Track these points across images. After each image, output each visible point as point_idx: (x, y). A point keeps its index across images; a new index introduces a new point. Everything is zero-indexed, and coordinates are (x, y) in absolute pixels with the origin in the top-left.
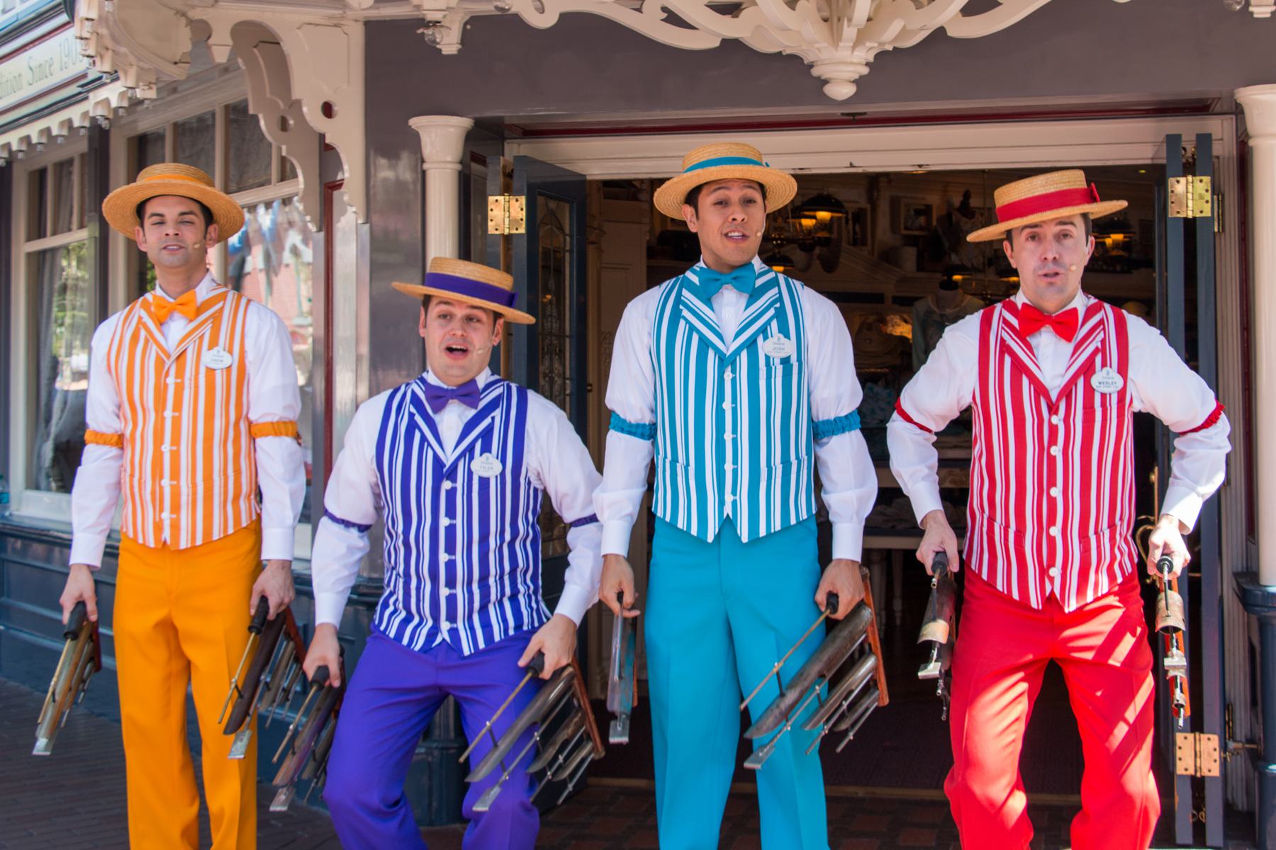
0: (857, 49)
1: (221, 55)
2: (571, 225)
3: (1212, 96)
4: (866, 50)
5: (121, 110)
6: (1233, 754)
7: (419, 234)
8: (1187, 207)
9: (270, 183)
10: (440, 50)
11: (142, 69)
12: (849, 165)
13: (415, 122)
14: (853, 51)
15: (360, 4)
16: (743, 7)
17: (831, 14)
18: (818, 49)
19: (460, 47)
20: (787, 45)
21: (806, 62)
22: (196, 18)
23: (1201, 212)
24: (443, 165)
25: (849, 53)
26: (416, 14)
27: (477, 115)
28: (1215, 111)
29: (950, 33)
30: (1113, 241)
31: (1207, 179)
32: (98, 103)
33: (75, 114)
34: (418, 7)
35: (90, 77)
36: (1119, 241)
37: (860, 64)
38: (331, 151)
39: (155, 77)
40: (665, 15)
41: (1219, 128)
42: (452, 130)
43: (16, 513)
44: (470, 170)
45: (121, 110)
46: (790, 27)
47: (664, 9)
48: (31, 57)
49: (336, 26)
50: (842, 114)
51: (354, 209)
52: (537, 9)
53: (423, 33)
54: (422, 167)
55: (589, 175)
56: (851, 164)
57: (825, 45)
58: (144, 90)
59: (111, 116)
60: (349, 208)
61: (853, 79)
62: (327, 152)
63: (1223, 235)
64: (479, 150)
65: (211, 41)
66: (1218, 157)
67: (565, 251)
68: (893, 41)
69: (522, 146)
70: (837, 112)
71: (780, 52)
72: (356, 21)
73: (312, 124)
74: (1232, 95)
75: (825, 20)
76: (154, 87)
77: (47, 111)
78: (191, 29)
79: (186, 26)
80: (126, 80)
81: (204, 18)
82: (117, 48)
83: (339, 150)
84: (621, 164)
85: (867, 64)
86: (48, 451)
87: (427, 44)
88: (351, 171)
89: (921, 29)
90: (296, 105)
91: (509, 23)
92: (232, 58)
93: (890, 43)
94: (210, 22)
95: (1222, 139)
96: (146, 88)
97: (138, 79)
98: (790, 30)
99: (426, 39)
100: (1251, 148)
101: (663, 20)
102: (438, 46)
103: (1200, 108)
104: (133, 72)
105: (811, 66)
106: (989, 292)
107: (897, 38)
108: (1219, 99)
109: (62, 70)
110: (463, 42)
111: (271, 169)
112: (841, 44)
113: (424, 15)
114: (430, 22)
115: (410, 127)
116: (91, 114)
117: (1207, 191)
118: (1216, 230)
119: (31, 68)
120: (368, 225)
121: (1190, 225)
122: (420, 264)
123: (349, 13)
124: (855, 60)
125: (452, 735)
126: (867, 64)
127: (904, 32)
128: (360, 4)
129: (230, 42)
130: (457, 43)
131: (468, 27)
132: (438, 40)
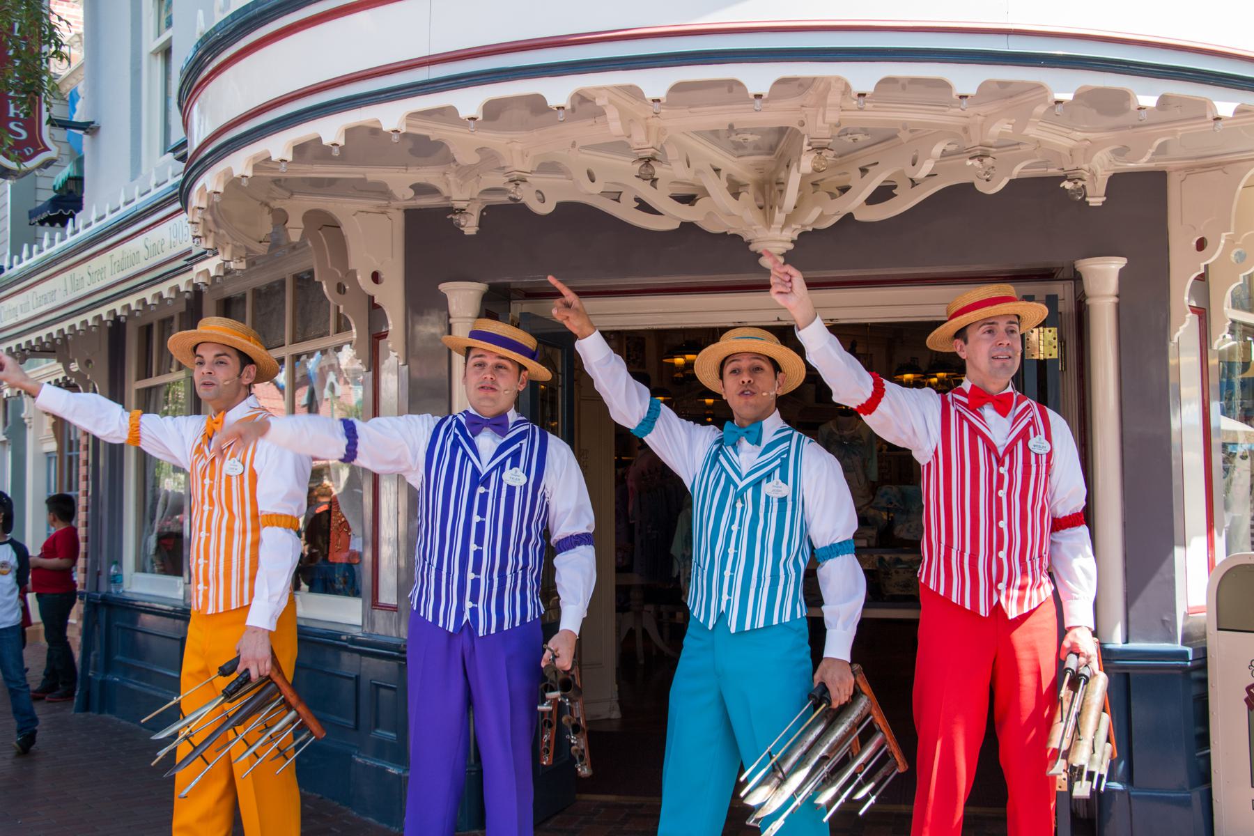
0: (785, 230)
1: (295, 236)
2: (562, 366)
5: (218, 278)
7: (446, 374)
8: (1039, 351)
9: (329, 335)
10: (463, 231)
11: (235, 246)
12: (776, 319)
13: (444, 287)
14: (782, 231)
15: (404, 196)
16: (697, 198)
18: (755, 230)
19: (478, 229)
21: (745, 240)
22: (276, 207)
23: (1050, 355)
25: (778, 233)
26: (445, 204)
27: (491, 281)
31: (1054, 330)
32: (200, 273)
33: (182, 282)
34: (448, 198)
35: (194, 253)
37: (787, 241)
38: (376, 310)
39: (245, 253)
41: (1062, 290)
42: (472, 293)
43: (127, 590)
45: (218, 278)
46: (733, 211)
47: (637, 199)
48: (147, 238)
49: (383, 213)
51: (396, 354)
52: (539, 200)
53: (452, 218)
54: (448, 322)
56: (778, 318)
57: (761, 227)
59: (209, 283)
60: (391, 353)
62: (375, 310)
63: (1065, 373)
64: (493, 309)
65: (287, 225)
66: (1061, 313)
67: (557, 386)
68: (812, 224)
69: (524, 305)
71: (726, 232)
72: (398, 209)
73: (364, 289)
74: (1074, 265)
75: (761, 208)
76: (244, 260)
77: (159, 280)
79: (269, 214)
80: (223, 255)
81: (282, 207)
82: (216, 231)
83: (385, 309)
85: (793, 242)
86: (152, 541)
88: (395, 323)
89: (835, 214)
90: (354, 273)
91: (518, 210)
92: (303, 236)
93: (809, 225)
94: (286, 210)
95: (1064, 299)
96: (238, 261)
97: (232, 257)
98: (734, 215)
100: (1088, 306)
101: (636, 208)
102: (462, 229)
103: (1046, 275)
104: (229, 249)
105: (749, 243)
107: (818, 220)
108: (1063, 268)
109: (171, 248)
110: (480, 225)
111: (329, 324)
112: (772, 226)
113: (453, 204)
114: (457, 209)
116: (194, 282)
117: (1055, 339)
118: (1060, 369)
119: (147, 247)
120: (407, 366)
121: (1042, 364)
123: (393, 203)
124: (785, 239)
125: (472, 761)
126: (793, 242)
127: (821, 217)
128: (404, 196)
129: (303, 226)
131: (485, 214)
132: (463, 224)
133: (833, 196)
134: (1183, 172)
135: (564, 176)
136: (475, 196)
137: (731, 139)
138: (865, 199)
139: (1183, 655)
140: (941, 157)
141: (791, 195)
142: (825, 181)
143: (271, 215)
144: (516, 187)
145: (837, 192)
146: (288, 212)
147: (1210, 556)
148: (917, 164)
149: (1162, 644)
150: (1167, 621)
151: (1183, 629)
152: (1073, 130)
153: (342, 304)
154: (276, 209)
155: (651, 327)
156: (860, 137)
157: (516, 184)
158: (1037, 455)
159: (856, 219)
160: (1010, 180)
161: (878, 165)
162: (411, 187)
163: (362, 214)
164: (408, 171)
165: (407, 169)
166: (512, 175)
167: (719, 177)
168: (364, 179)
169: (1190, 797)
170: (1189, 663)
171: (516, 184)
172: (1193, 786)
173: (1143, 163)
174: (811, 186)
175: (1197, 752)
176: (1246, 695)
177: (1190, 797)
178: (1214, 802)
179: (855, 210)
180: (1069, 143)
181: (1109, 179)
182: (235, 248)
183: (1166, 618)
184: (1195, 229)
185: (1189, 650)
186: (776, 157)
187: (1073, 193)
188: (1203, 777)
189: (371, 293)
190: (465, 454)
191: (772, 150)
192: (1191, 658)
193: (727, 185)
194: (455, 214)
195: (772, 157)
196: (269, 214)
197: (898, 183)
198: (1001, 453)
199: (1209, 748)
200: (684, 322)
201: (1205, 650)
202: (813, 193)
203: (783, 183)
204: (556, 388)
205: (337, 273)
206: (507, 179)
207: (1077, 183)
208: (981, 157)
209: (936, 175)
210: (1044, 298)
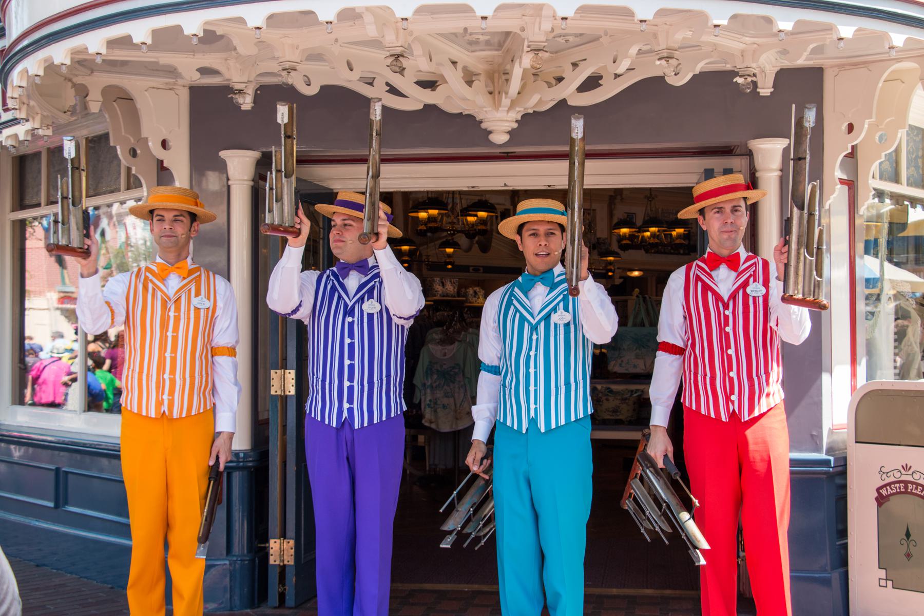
0: (511, 112)
3: (734, 144)
4: (516, 112)
6: (742, 560)
12: (503, 185)
13: (223, 154)
16: (438, 84)
17: (494, 90)
18: (486, 111)
19: (253, 105)
20: (466, 109)
21: (477, 119)
22: (78, 82)
24: (241, 182)
25: (505, 114)
27: (264, 150)
28: (736, 153)
29: (570, 103)
30: (677, 233)
36: (681, 233)
37: (512, 121)
39: (51, 122)
40: (388, 88)
42: (248, 159)
44: (259, 186)
46: (469, 98)
47: (387, 84)
49: (170, 89)
50: (500, 153)
54: (227, 183)
55: (335, 189)
56: (505, 184)
57: (490, 109)
58: (44, 129)
61: (507, 131)
65: (88, 98)
67: (320, 238)
70: (497, 151)
71: (461, 113)
72: (184, 86)
73: (153, 153)
75: (491, 93)
76: (51, 128)
78: (75, 90)
79: (72, 88)
81: (84, 82)
84: (355, 182)
85: (517, 121)
87: (235, 104)
93: (531, 108)
96: (45, 128)
97: (42, 123)
98: (469, 100)
99: (234, 101)
104: (38, 118)
105: (481, 122)
106: (593, 267)
110: (255, 102)
112: (500, 109)
113: (233, 85)
114: (236, 90)
115: (220, 156)
122: (226, 246)
123: (180, 81)
126: (517, 121)
128: (191, 77)
129: (101, 99)
130: (251, 103)
133: (550, 85)
134: (836, 68)
135: (327, 64)
136: (252, 79)
137: (465, 38)
138: (576, 87)
139: (826, 463)
140: (637, 54)
141: (515, 84)
142: (544, 72)
143: (73, 89)
144: (288, 75)
145: (554, 82)
146: (89, 88)
147: (853, 383)
148: (617, 61)
149: (810, 454)
150: (815, 435)
151: (827, 444)
152: (743, 35)
153: (134, 166)
154: (78, 84)
155: (399, 190)
156: (571, 39)
157: (288, 72)
158: (754, 298)
159: (569, 104)
160: (694, 75)
161: (587, 60)
162: (197, 70)
163: (154, 89)
164: (196, 57)
165: (194, 55)
166: (284, 65)
167: (456, 69)
168: (157, 63)
169: (831, 577)
170: (831, 469)
171: (288, 72)
172: (833, 568)
173: (801, 62)
174: (532, 75)
175: (838, 541)
176: (876, 495)
177: (831, 577)
178: (850, 581)
179: (568, 96)
180: (742, 46)
181: (776, 74)
182: (44, 118)
183: (814, 433)
184: (844, 117)
185: (832, 458)
186: (502, 53)
187: (744, 87)
188: (842, 560)
189: (161, 158)
190: (340, 297)
191: (500, 45)
192: (832, 466)
193: (462, 75)
194: (236, 94)
195: (499, 53)
196: (72, 88)
197: (603, 74)
198: (726, 299)
199: (847, 539)
200: (426, 186)
201: (845, 459)
202: (534, 82)
203: (508, 73)
204: (318, 240)
205: (130, 140)
206: (280, 68)
207: (746, 79)
208: (668, 58)
209: (634, 69)
210: (722, 171)
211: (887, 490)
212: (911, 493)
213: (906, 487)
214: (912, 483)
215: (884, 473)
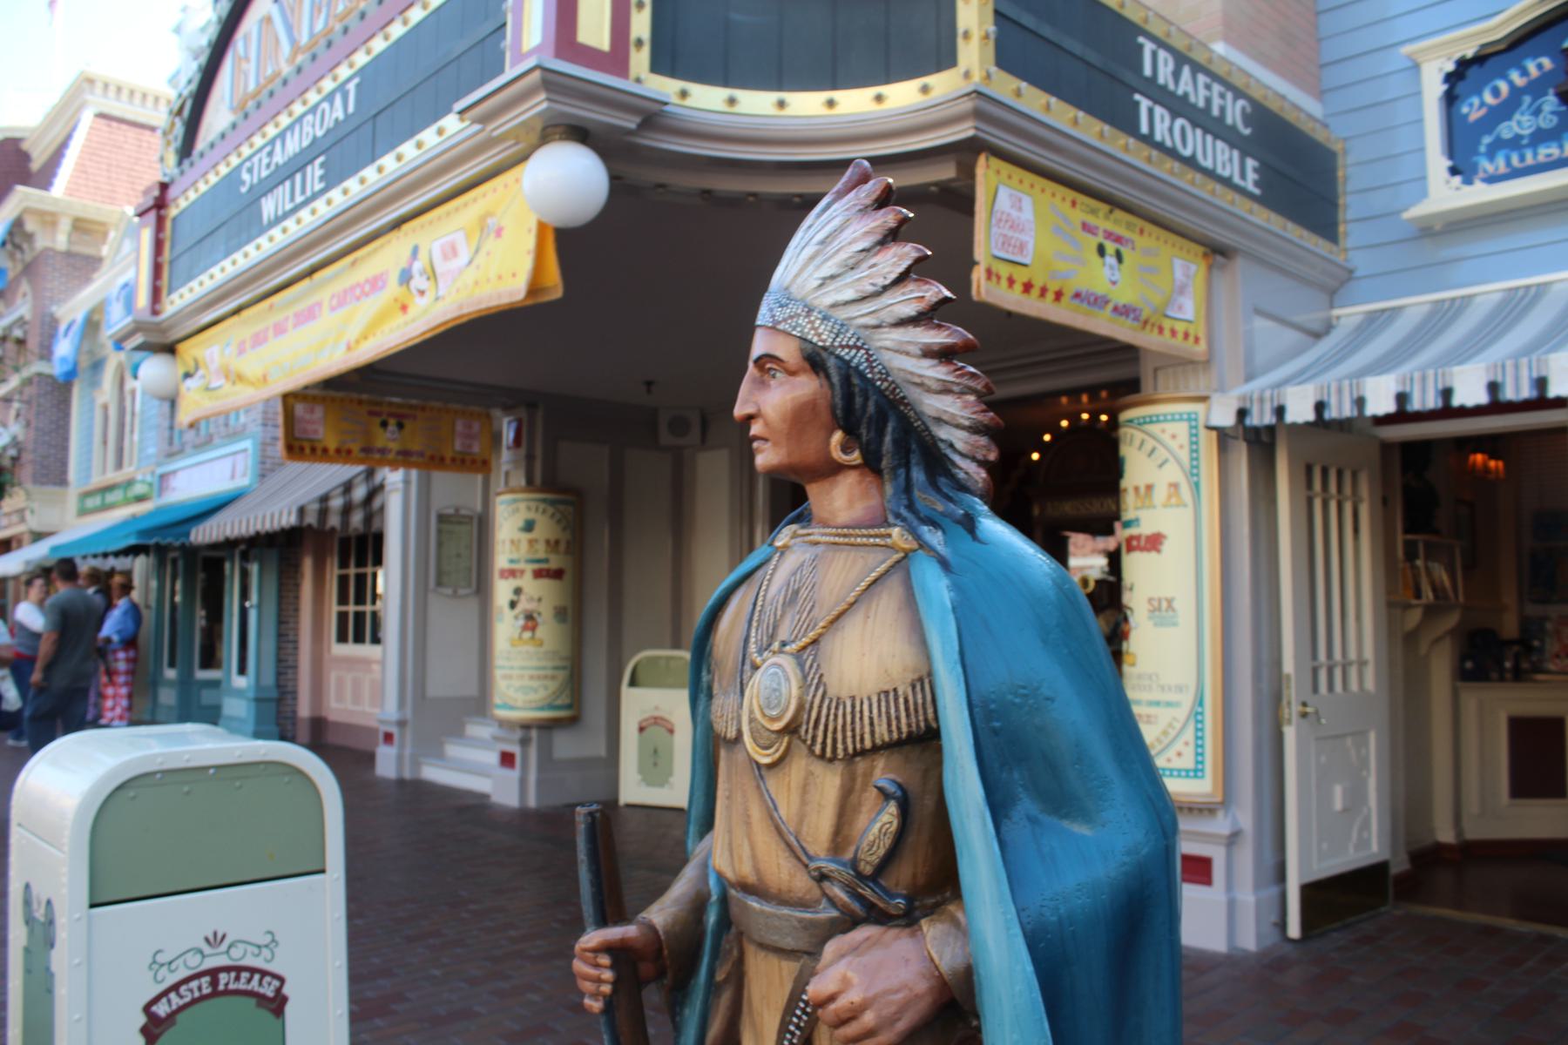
176: (142, 1020)
211: (169, 1001)
212: (227, 992)
213: (214, 983)
214: (228, 969)
215: (162, 965)
